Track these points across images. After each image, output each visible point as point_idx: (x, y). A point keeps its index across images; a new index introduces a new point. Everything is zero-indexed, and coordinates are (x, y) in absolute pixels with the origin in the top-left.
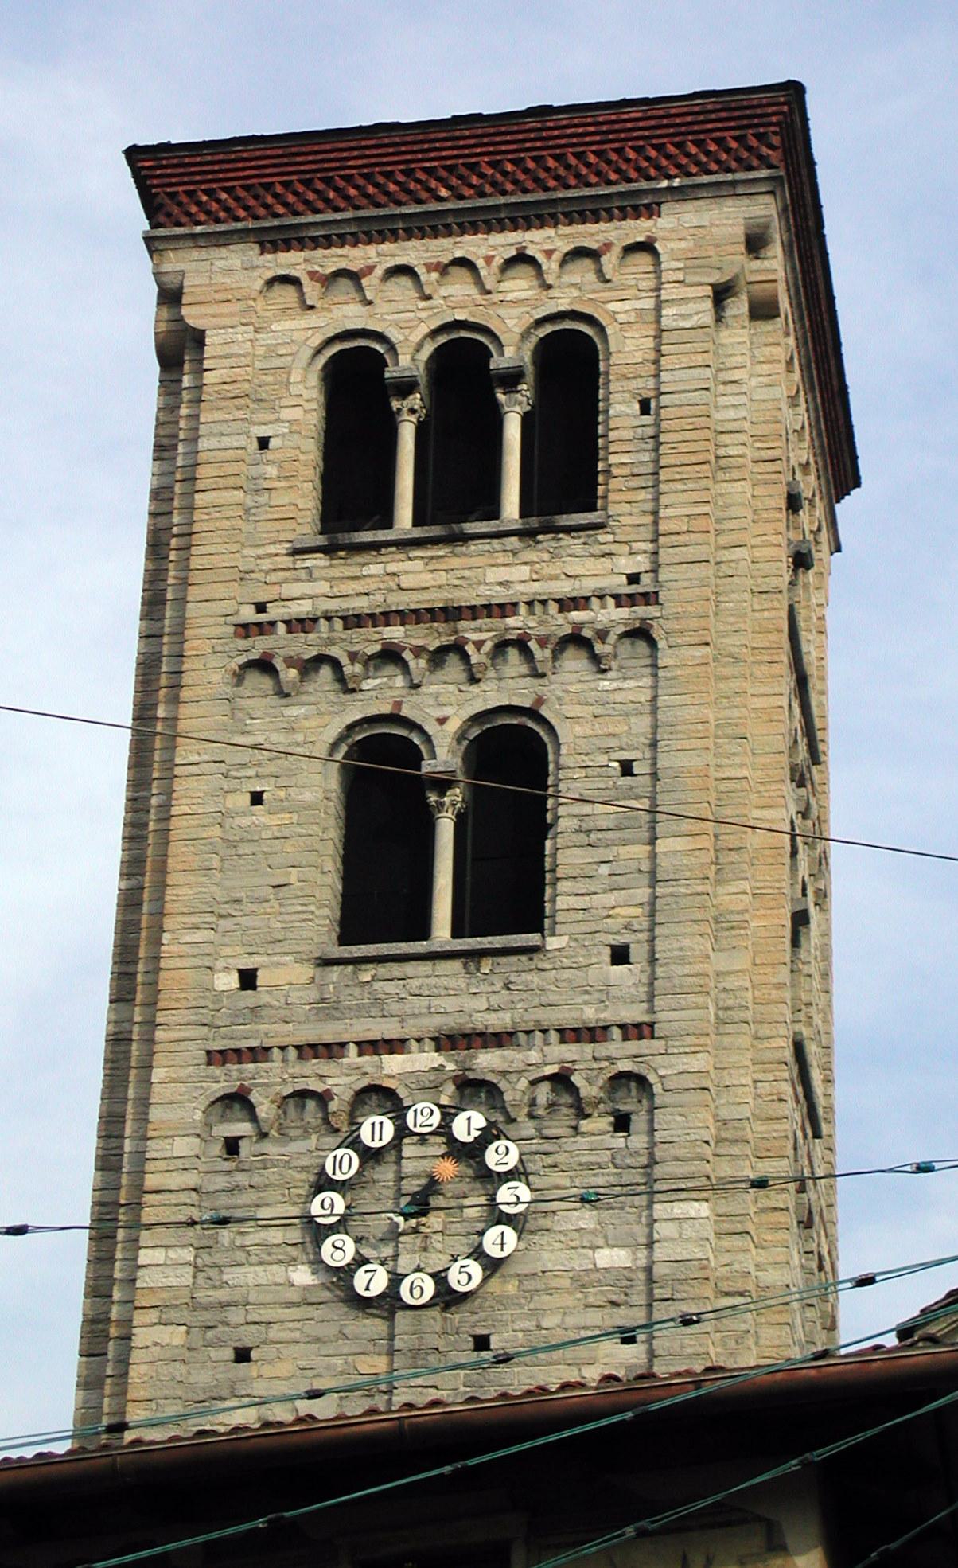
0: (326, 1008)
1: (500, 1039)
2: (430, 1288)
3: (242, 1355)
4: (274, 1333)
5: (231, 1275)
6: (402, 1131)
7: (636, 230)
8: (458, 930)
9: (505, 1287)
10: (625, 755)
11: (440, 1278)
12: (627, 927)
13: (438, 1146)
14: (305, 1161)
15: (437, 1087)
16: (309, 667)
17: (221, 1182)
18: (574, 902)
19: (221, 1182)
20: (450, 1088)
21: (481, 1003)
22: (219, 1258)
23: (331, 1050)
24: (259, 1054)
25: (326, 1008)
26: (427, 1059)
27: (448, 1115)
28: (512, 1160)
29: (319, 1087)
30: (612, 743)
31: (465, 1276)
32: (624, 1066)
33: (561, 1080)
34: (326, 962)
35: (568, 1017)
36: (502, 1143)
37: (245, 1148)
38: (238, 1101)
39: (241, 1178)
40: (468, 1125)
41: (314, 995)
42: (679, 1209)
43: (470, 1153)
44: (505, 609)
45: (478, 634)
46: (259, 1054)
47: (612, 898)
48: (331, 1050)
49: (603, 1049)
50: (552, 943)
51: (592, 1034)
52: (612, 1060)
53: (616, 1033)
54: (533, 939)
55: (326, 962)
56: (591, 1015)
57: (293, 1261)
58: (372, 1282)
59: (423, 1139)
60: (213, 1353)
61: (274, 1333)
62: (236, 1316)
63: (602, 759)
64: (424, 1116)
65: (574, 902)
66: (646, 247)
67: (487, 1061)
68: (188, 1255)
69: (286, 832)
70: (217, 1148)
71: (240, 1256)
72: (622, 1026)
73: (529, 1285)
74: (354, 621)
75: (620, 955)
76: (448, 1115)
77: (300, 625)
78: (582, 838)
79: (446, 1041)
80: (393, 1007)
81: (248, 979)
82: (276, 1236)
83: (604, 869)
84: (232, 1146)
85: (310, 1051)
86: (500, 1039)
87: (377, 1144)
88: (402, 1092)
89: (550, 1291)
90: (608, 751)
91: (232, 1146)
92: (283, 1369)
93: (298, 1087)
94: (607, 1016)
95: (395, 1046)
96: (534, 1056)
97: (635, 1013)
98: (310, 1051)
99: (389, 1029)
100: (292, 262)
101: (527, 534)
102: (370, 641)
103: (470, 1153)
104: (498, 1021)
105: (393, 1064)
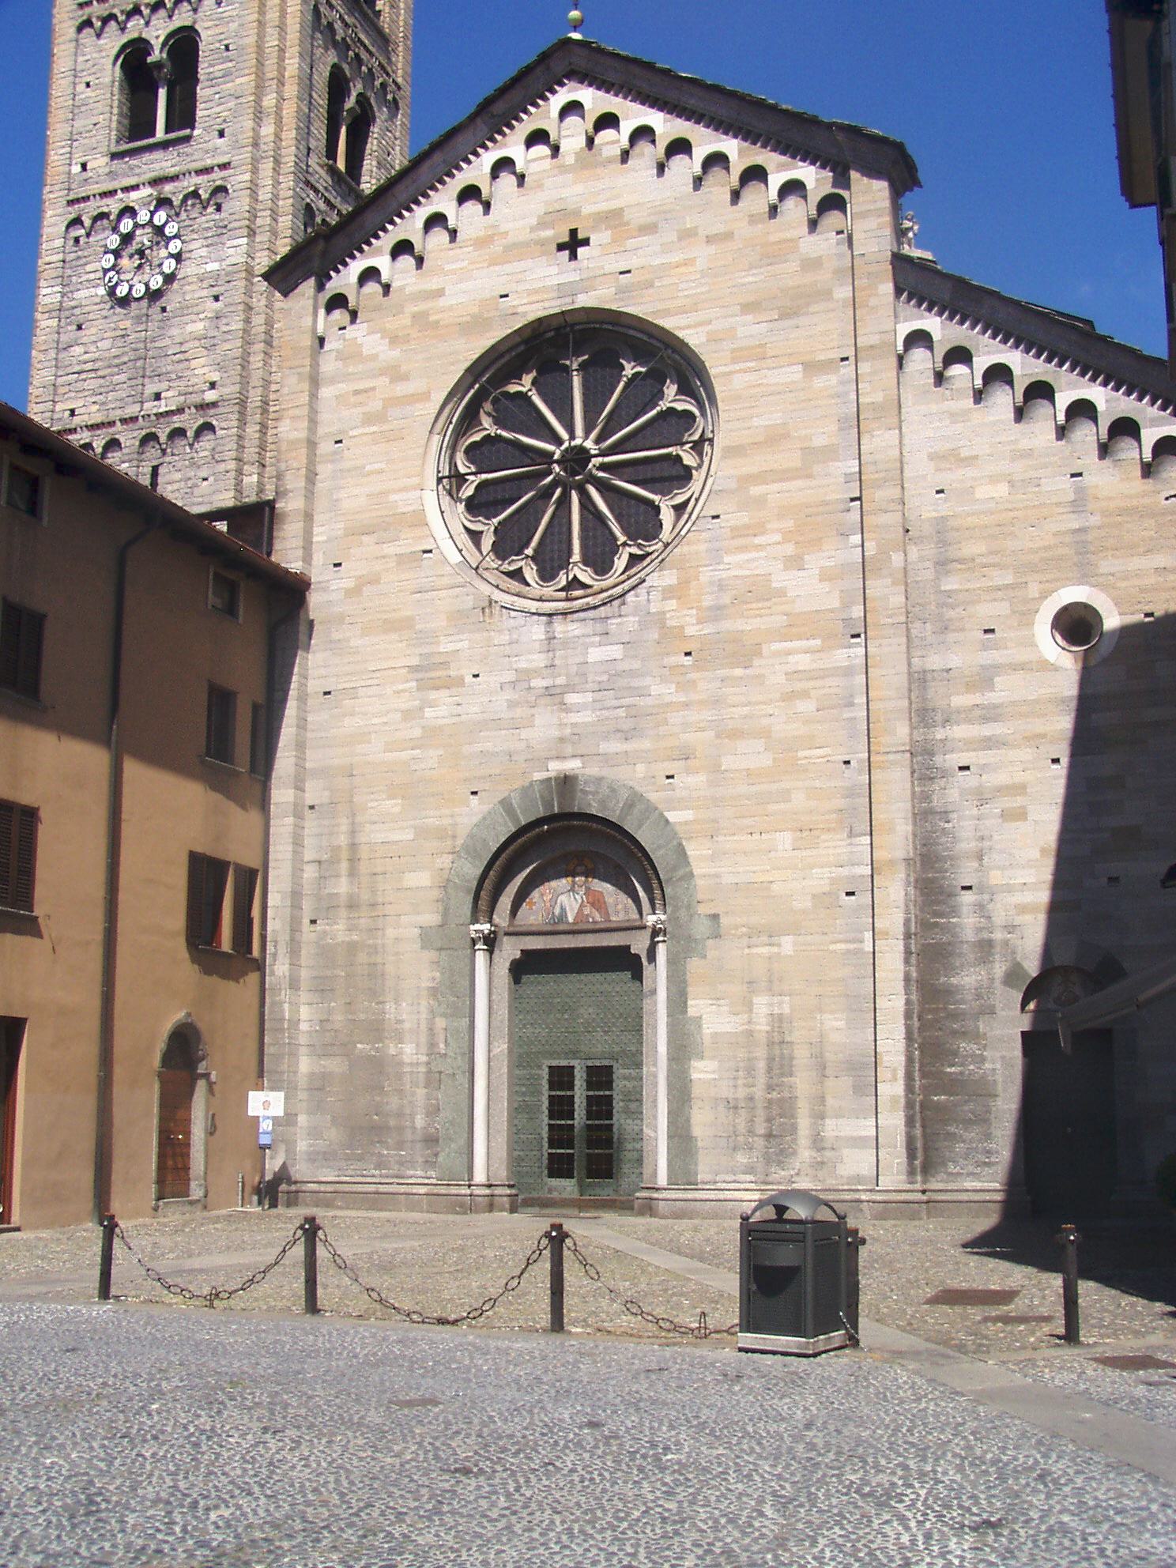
0: (112, 175)
1: (174, 178)
2: (143, 289)
3: (79, 328)
4: (91, 316)
5: (76, 295)
6: (136, 226)
8: (167, 132)
9: (175, 285)
10: (226, 42)
11: (147, 285)
12: (225, 121)
13: (149, 230)
14: (103, 243)
15: (149, 203)
17: (73, 256)
18: (206, 113)
19: (73, 256)
20: (155, 202)
21: (169, 164)
22: (72, 288)
23: (112, 193)
24: (86, 199)
25: (112, 175)
26: (146, 191)
27: (152, 213)
28: (175, 231)
29: (105, 210)
30: (222, 37)
31: (156, 282)
32: (218, 183)
33: (195, 194)
34: (115, 156)
35: (199, 165)
36: (170, 224)
37: (82, 241)
38: (77, 222)
39: (80, 253)
40: (160, 217)
41: (107, 170)
42: (235, 242)
43: (159, 231)
46: (86, 199)
47: (218, 109)
48: (112, 193)
49: (213, 176)
50: (196, 132)
51: (207, 171)
52: (214, 181)
53: (216, 168)
54: (187, 132)
55: (115, 156)
56: (209, 162)
57: (99, 285)
58: (122, 291)
59: (143, 226)
60: (69, 328)
61: (91, 316)
62: (77, 311)
63: (218, 45)
64: (143, 216)
65: (206, 113)
67: (168, 188)
68: (58, 289)
69: (98, 98)
70: (71, 242)
71: (79, 286)
72: (219, 166)
73: (182, 282)
75: (221, 134)
76: (152, 213)
78: (210, 83)
79: (155, 182)
80: (137, 171)
81: (84, 166)
82: (92, 276)
83: (217, 96)
84: (77, 240)
85: (105, 195)
86: (174, 178)
87: (126, 231)
88: (137, 208)
89: (189, 284)
90: (220, 41)
91: (77, 240)
92: (93, 330)
93: (100, 210)
94: (215, 162)
95: (135, 188)
96: (186, 184)
97: (224, 160)
98: (105, 195)
99: (132, 181)
104: (173, 171)
105: (134, 195)
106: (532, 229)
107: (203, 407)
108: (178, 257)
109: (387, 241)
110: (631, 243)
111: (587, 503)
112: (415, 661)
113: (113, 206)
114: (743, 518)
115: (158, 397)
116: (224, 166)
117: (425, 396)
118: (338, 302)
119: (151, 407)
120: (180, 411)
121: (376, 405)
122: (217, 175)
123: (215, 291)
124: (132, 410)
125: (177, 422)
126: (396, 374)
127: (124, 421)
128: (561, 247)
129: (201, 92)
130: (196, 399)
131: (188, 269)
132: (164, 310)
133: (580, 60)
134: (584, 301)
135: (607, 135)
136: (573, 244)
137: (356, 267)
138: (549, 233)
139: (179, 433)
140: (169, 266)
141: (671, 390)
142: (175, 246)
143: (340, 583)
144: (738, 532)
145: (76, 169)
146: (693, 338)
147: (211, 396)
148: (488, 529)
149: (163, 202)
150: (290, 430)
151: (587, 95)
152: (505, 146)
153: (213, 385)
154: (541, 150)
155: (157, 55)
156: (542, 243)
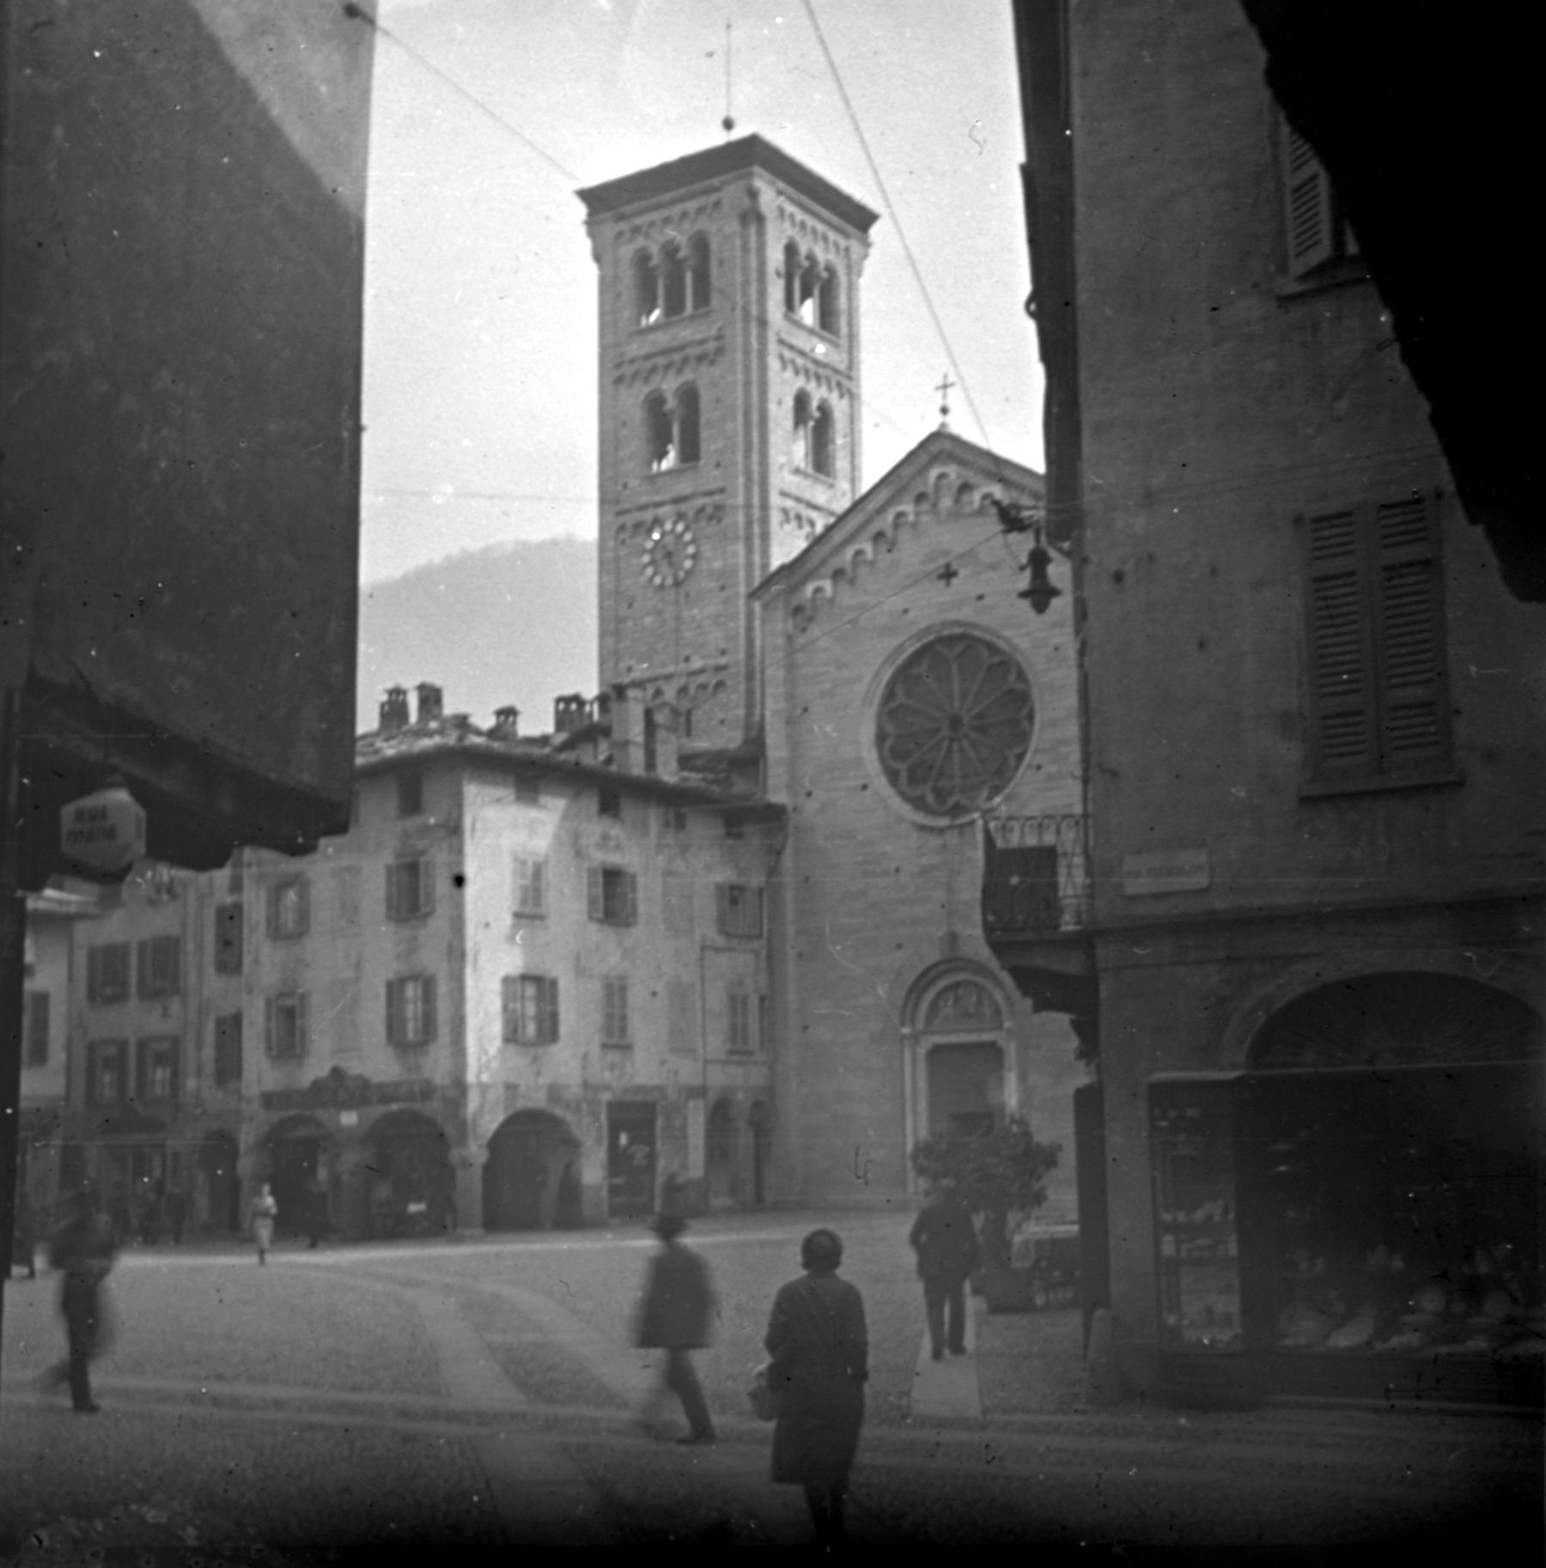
7: (713, 198)
16: (635, 375)
23: (644, 508)
27: (675, 523)
38: (622, 528)
40: (680, 527)
44: (682, 348)
45: (677, 357)
48: (644, 508)
51: (710, 493)
58: (658, 580)
64: (668, 526)
66: (717, 204)
67: (683, 507)
74: (648, 357)
75: (718, 465)
76: (675, 523)
77: (632, 361)
79: (677, 501)
91: (623, 542)
100: (623, 226)
101: (692, 318)
102: (649, 364)
103: (681, 535)
104: (688, 491)
106: (923, 563)
107: (719, 669)
108: (695, 557)
109: (828, 569)
110: (985, 576)
111: (962, 750)
112: (860, 858)
113: (648, 516)
114: (1053, 769)
115: (687, 659)
116: (722, 491)
117: (859, 679)
118: (798, 610)
119: (683, 667)
120: (702, 671)
121: (827, 686)
122: (717, 498)
123: (722, 582)
124: (670, 669)
125: (701, 679)
126: (841, 666)
127: (669, 677)
128: (941, 577)
129: (704, 434)
130: (711, 662)
131: (704, 566)
132: (687, 595)
133: (947, 445)
134: (953, 615)
135: (966, 498)
136: (948, 575)
137: (809, 588)
138: (931, 567)
139: (703, 687)
140: (688, 564)
141: (1012, 676)
142: (691, 550)
143: (811, 806)
144: (1050, 777)
145: (620, 488)
146: (1023, 644)
147: (723, 660)
148: (902, 766)
149: (680, 516)
150: (773, 707)
151: (952, 470)
152: (901, 503)
153: (723, 652)
154: (925, 506)
155: (671, 403)
156: (927, 575)
